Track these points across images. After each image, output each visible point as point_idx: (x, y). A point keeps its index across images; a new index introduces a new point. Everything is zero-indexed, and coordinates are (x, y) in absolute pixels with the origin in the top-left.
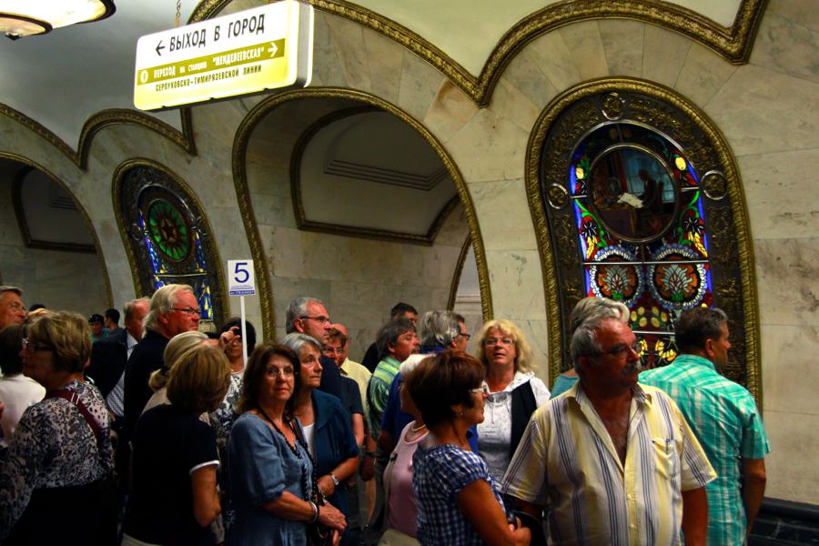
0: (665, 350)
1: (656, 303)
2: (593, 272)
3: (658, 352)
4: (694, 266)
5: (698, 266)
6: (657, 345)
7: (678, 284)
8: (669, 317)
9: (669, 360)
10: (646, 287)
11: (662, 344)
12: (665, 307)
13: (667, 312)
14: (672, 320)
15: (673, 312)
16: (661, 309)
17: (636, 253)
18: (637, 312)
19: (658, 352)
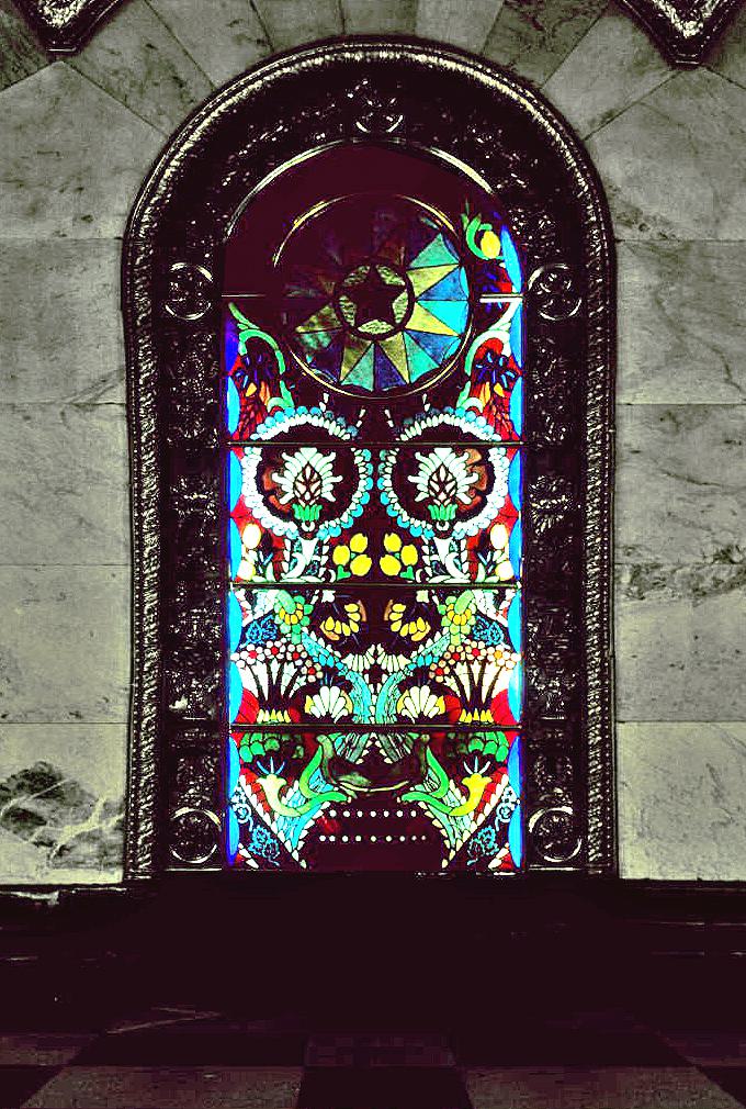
0: (407, 619)
1: (391, 526)
2: (253, 457)
3: (391, 622)
4: (486, 455)
5: (492, 451)
6: (388, 610)
7: (448, 487)
8: (421, 553)
9: (413, 638)
10: (375, 493)
11: (400, 608)
12: (415, 533)
13: (418, 543)
14: (426, 559)
15: (432, 543)
16: (407, 538)
17: (359, 423)
18: (348, 545)
19: (391, 622)
